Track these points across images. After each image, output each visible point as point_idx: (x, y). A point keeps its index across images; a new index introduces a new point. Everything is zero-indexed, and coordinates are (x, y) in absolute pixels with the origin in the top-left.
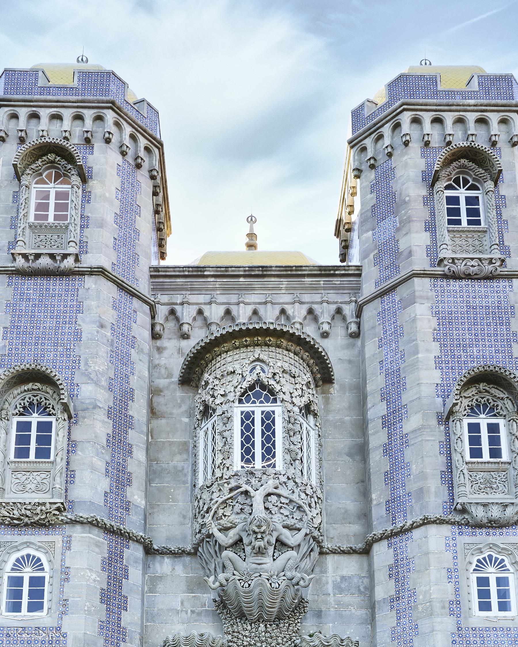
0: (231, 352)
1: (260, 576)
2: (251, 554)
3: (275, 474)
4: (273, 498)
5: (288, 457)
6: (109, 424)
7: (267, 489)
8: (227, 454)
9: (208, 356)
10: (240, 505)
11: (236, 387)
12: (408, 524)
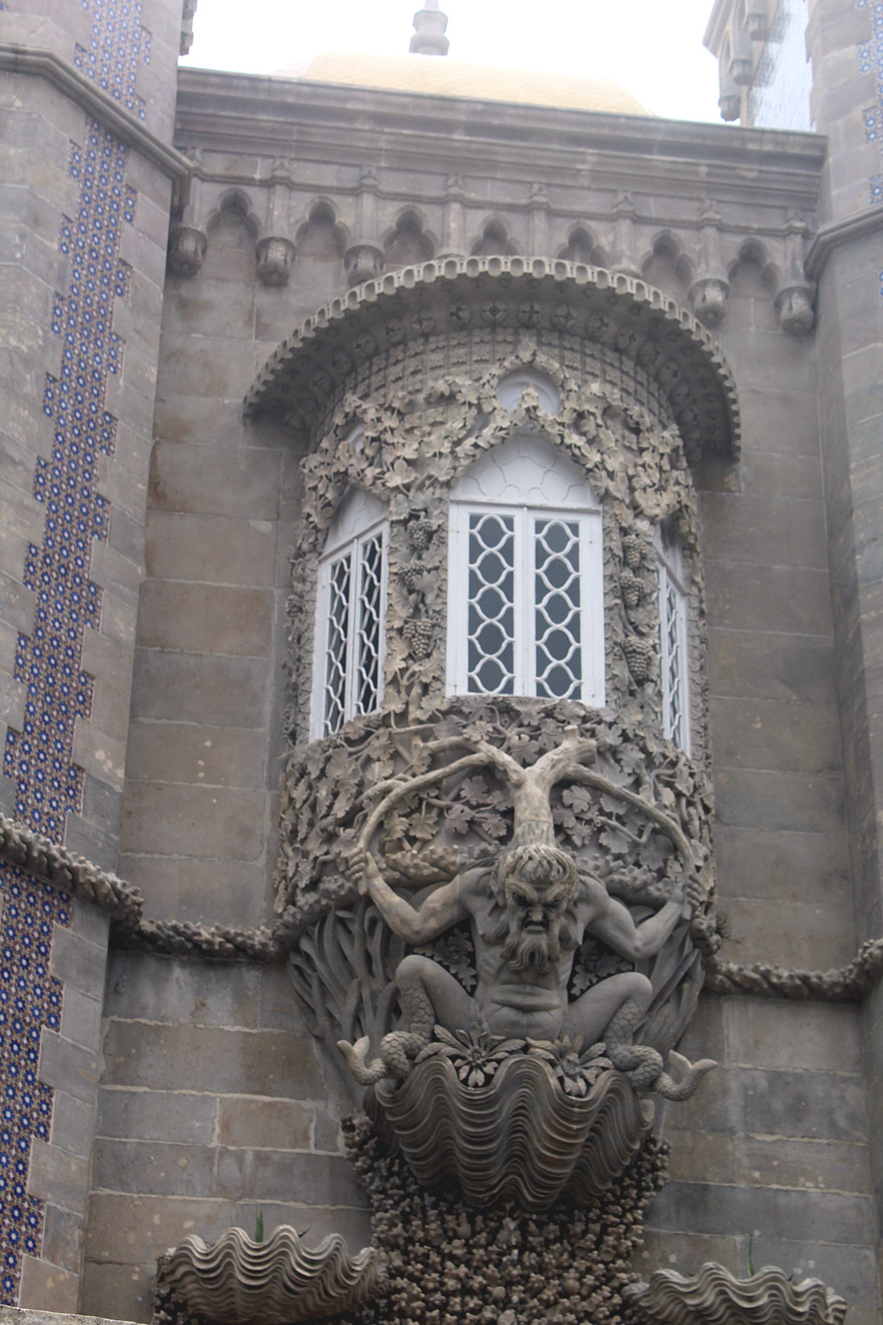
0: (442, 338)
1: (526, 1049)
2: (500, 971)
3: (585, 719)
4: (579, 797)
6: (38, 514)
7: (560, 766)
8: (424, 641)
9: (362, 341)
10: (467, 809)
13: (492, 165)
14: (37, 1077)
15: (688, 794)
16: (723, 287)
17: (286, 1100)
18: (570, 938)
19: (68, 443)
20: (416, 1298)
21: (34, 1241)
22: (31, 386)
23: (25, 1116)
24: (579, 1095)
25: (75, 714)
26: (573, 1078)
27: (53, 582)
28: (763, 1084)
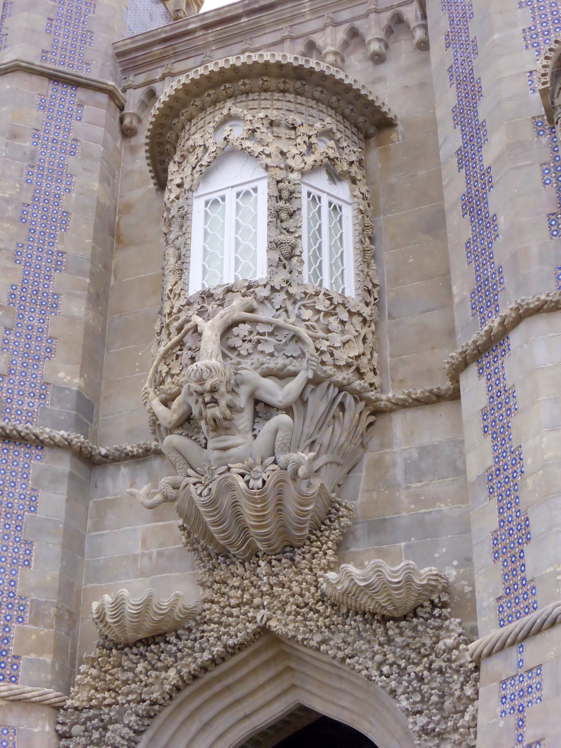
1: (229, 469)
3: (249, 287)
4: (243, 329)
5: (276, 255)
10: (189, 352)
11: (196, 166)
12: (496, 324)
13: (263, 27)
14: (22, 538)
15: (324, 309)
16: (379, 40)
17: (171, 522)
18: (236, 405)
19: (37, 232)
20: (215, 612)
21: (22, 618)
22: (11, 211)
23: (15, 558)
24: (259, 489)
25: (45, 359)
26: (257, 479)
27: (28, 300)
28: (415, 455)
